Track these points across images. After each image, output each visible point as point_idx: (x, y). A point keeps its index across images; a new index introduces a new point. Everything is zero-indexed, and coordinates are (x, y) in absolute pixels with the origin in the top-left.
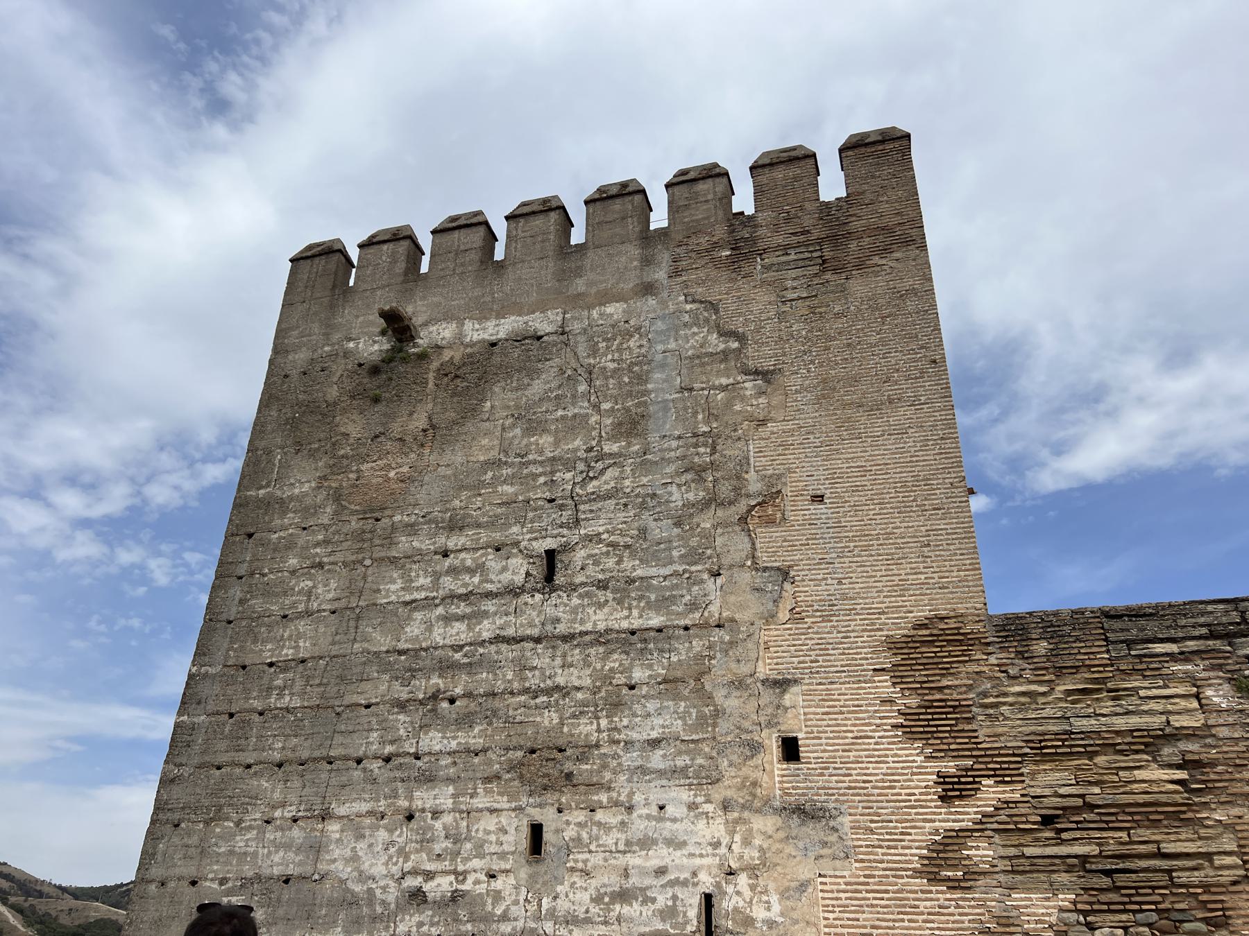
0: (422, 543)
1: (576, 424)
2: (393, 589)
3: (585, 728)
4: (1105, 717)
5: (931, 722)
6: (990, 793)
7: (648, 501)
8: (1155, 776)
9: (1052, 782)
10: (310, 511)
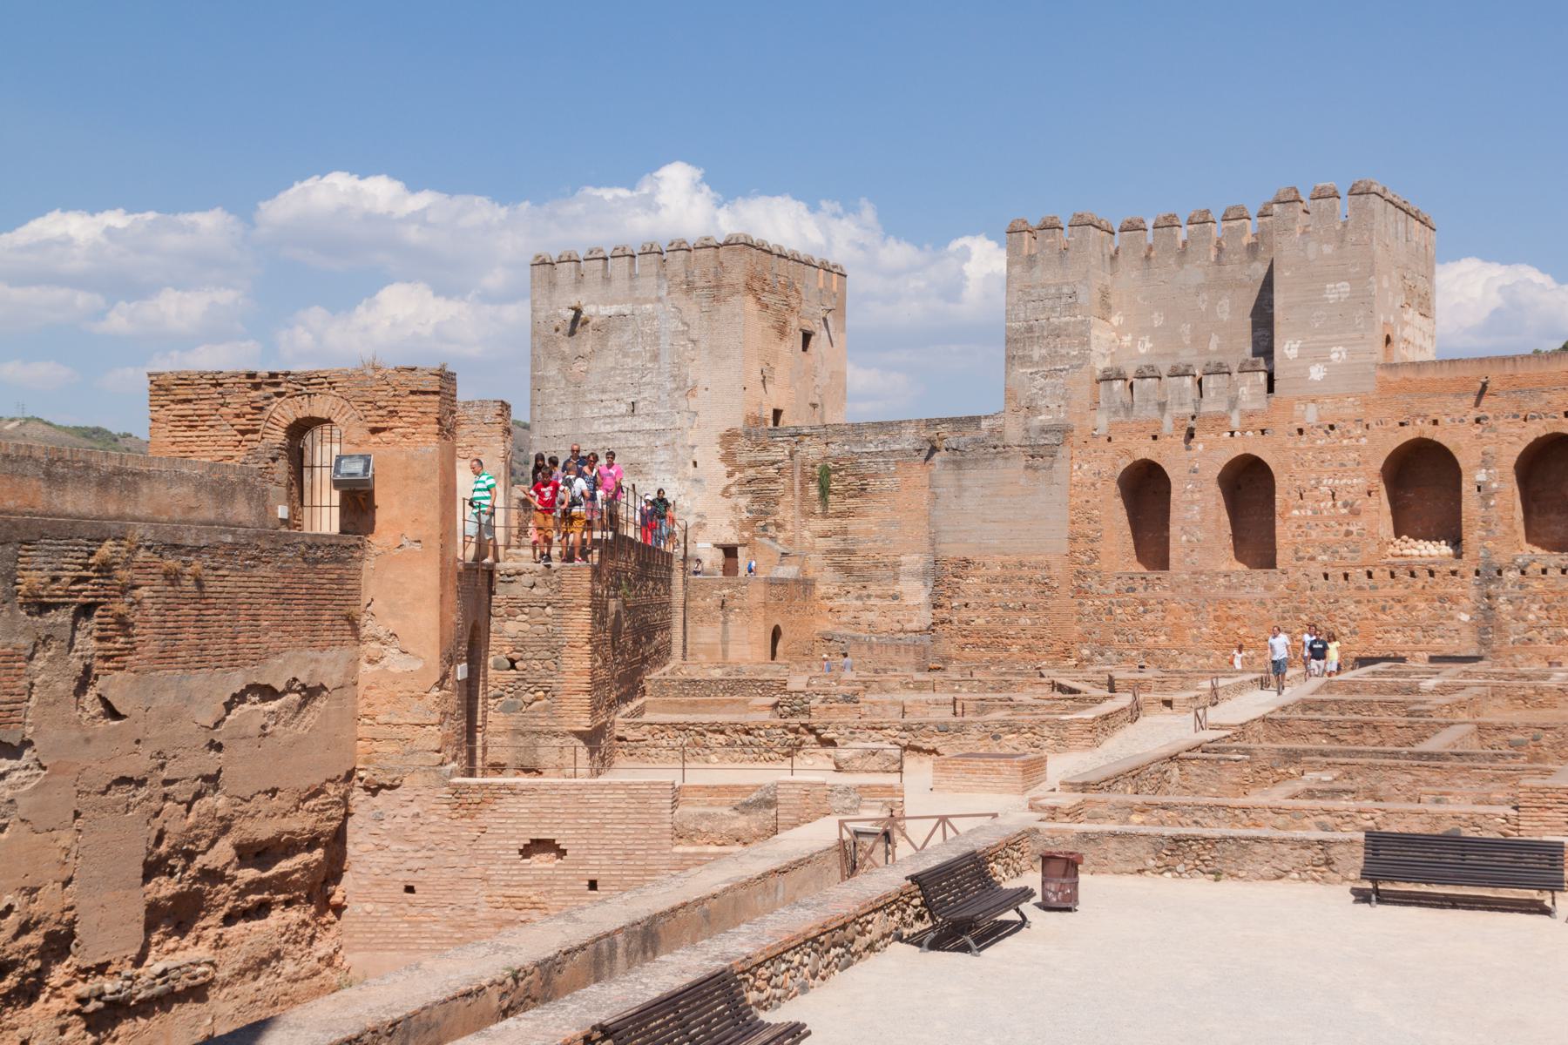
0: (594, 397)
1: (637, 355)
2: (587, 413)
3: (645, 458)
4: (764, 456)
5: (728, 457)
6: (738, 475)
7: (660, 387)
8: (771, 471)
9: (751, 472)
10: (557, 382)
